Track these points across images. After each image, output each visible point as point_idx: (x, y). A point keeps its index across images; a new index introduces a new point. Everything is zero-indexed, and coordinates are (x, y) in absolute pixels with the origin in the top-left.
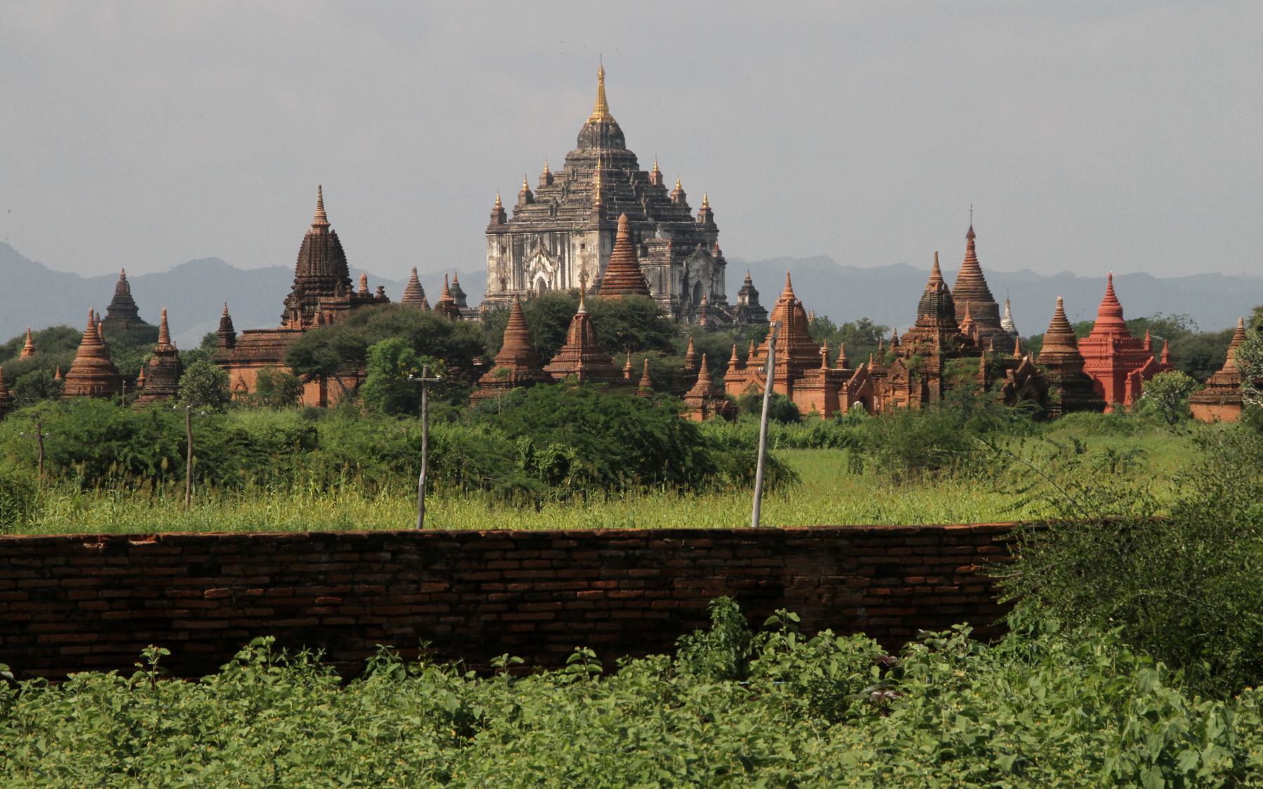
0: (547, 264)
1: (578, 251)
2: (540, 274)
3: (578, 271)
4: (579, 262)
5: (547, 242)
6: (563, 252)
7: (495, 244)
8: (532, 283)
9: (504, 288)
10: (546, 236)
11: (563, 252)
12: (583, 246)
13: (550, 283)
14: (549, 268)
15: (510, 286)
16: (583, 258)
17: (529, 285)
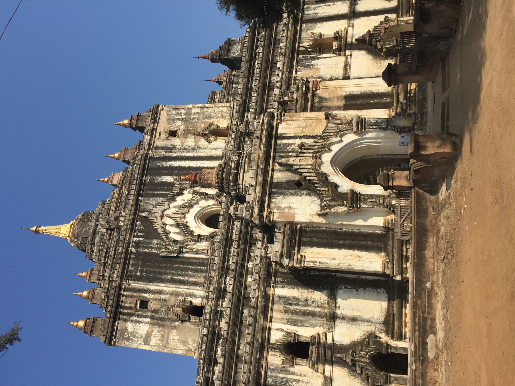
0: (180, 200)
1: (177, 142)
2: (190, 219)
3: (202, 142)
4: (190, 141)
5: (153, 201)
6: (170, 171)
7: (130, 326)
8: (200, 238)
9: (197, 311)
10: (143, 203)
11: (170, 171)
12: (173, 134)
13: (206, 196)
14: (187, 196)
15: (198, 296)
16: (187, 133)
17: (203, 245)
